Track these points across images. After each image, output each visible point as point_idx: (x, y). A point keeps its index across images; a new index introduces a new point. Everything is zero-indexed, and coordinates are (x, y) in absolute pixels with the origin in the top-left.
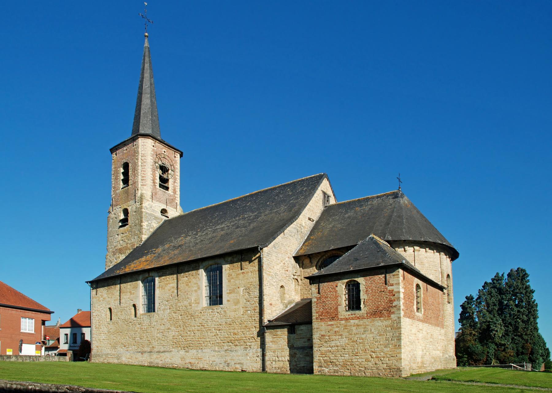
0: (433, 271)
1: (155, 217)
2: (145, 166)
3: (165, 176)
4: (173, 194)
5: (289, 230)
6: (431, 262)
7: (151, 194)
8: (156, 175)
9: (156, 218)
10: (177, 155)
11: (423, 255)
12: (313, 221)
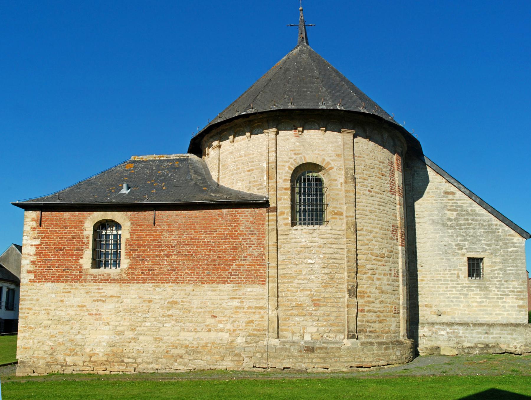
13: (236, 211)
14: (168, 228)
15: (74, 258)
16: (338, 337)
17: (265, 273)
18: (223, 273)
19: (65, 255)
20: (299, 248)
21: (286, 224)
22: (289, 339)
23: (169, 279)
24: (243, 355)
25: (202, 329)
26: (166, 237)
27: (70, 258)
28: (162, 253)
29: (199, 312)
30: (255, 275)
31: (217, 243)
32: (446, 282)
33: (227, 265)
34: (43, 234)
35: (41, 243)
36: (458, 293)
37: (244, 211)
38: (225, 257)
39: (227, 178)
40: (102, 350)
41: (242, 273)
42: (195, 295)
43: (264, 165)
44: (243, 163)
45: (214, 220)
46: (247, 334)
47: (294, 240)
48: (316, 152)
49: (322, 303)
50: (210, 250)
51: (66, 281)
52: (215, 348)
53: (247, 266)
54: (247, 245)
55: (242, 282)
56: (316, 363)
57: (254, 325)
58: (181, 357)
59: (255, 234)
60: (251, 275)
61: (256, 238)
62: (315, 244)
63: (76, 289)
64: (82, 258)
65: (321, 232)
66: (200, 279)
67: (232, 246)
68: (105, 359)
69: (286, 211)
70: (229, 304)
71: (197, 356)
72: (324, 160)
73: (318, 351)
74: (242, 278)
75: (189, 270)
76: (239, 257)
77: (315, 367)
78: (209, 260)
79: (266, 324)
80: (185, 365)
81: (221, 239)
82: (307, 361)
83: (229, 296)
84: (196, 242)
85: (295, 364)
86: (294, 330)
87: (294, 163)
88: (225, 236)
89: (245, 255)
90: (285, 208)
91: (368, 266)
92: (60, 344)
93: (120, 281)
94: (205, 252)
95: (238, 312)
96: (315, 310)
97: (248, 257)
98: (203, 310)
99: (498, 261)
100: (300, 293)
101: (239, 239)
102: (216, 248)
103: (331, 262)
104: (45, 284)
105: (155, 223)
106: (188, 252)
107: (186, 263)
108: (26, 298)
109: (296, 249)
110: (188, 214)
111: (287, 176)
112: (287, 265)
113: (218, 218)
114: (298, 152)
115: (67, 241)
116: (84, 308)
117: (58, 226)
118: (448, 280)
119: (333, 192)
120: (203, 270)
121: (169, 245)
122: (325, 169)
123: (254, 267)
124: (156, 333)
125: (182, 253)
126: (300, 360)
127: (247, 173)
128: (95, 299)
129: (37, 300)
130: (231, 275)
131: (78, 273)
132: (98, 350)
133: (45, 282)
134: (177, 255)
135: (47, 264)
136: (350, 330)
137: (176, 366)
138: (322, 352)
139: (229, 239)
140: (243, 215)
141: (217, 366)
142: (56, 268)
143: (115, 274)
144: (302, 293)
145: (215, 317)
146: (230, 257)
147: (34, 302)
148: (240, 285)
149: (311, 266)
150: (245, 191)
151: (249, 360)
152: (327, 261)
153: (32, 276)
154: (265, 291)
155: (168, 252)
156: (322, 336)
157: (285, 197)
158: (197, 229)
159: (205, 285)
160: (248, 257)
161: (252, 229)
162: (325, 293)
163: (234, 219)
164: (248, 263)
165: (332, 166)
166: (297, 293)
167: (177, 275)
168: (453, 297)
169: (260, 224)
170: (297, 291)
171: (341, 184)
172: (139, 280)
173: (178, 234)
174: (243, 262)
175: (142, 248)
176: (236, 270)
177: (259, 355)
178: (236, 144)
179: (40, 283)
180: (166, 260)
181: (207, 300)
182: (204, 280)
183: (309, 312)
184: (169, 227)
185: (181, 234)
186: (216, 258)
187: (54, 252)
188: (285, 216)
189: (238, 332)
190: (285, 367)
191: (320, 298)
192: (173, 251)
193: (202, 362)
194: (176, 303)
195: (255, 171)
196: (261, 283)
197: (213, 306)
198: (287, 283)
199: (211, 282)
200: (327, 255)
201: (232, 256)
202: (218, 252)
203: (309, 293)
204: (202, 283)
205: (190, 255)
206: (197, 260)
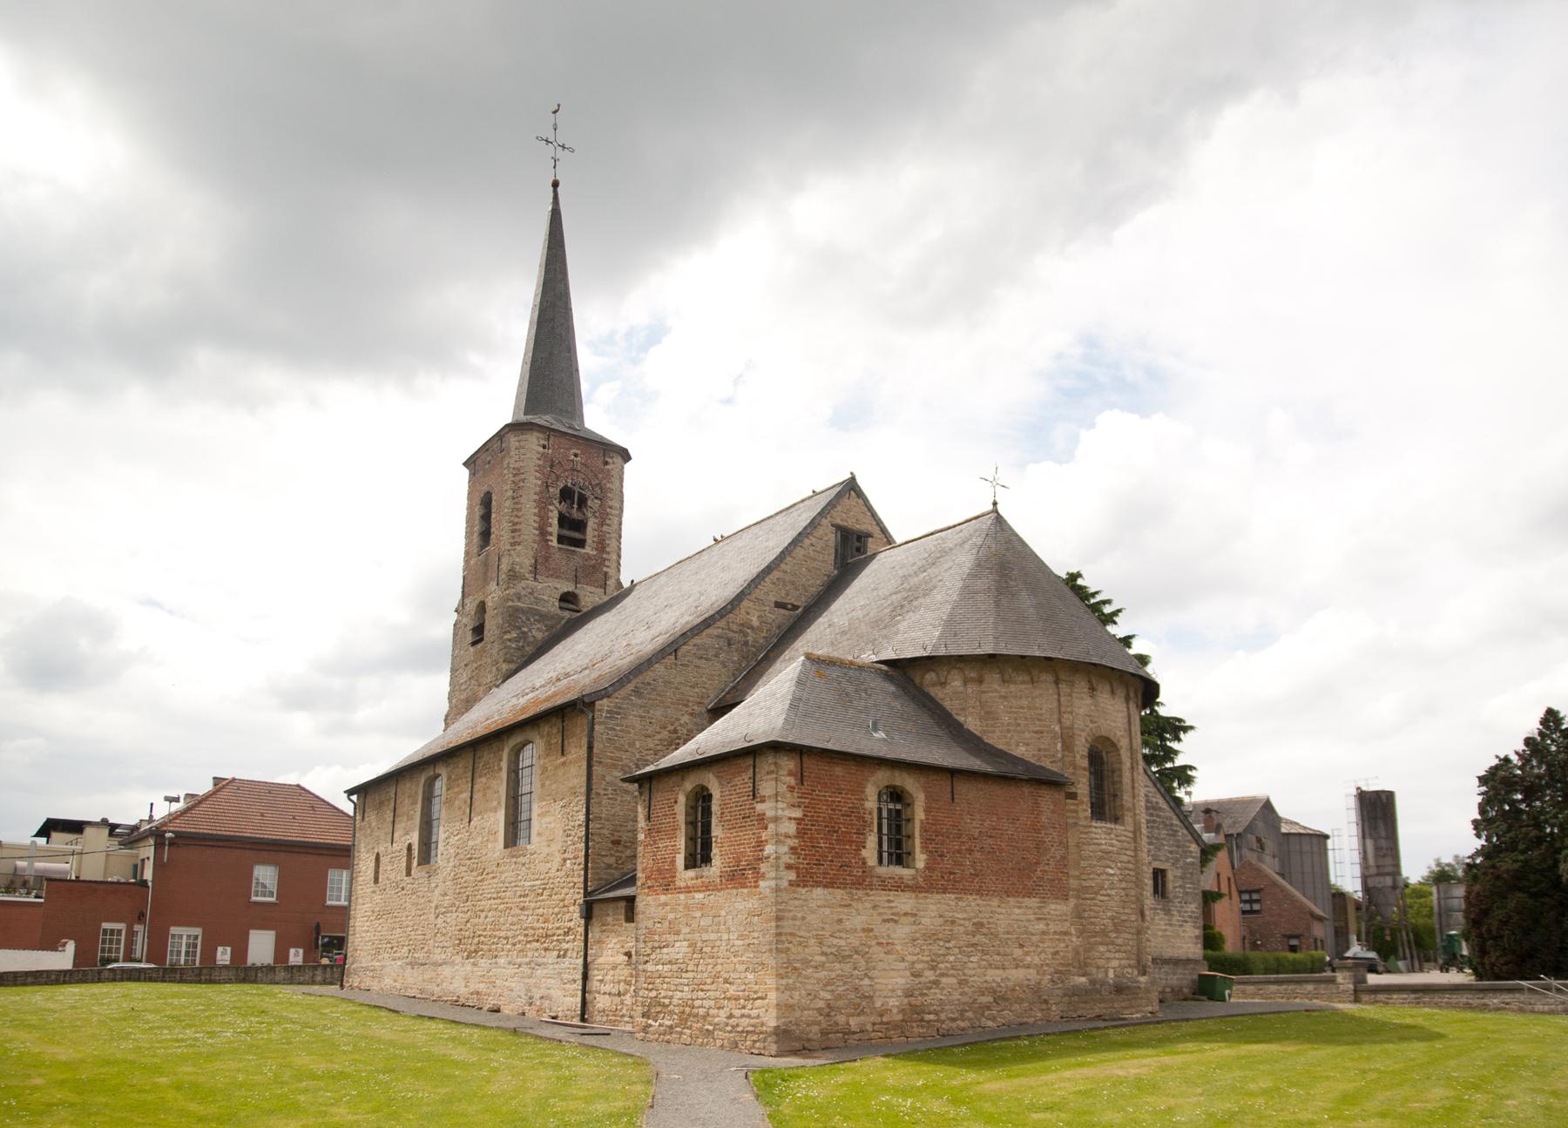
0: (1027, 735)
1: (541, 616)
2: (521, 496)
3: (575, 514)
4: (595, 553)
5: (694, 645)
6: (1023, 708)
7: (533, 561)
8: (550, 514)
9: (543, 617)
10: (612, 458)
11: (996, 691)
12: (795, 607)
15: (854, 847)
19: (840, 840)
21: (1086, 818)
27: (847, 847)
28: (964, 848)
34: (807, 801)
35: (804, 815)
39: (998, 734)
40: (896, 1003)
44: (1026, 719)
50: (1014, 846)
51: (843, 886)
63: (860, 899)
64: (864, 847)
68: (900, 1017)
70: (1037, 927)
72: (1116, 734)
79: (1070, 955)
92: (839, 997)
93: (915, 888)
96: (1116, 938)
99: (1179, 874)
104: (814, 889)
105: (953, 799)
108: (786, 915)
115: (843, 815)
116: (871, 934)
117: (828, 787)
124: (961, 973)
128: (886, 917)
129: (803, 918)
131: (860, 874)
132: (891, 1004)
133: (813, 886)
135: (814, 855)
142: (829, 863)
143: (909, 877)
147: (798, 923)
153: (792, 876)
172: (939, 889)
174: (1046, 868)
175: (940, 837)
179: (806, 889)
187: (824, 834)
188: (1084, 807)
195: (1045, 734)
200: (1124, 865)
204: (1008, 896)
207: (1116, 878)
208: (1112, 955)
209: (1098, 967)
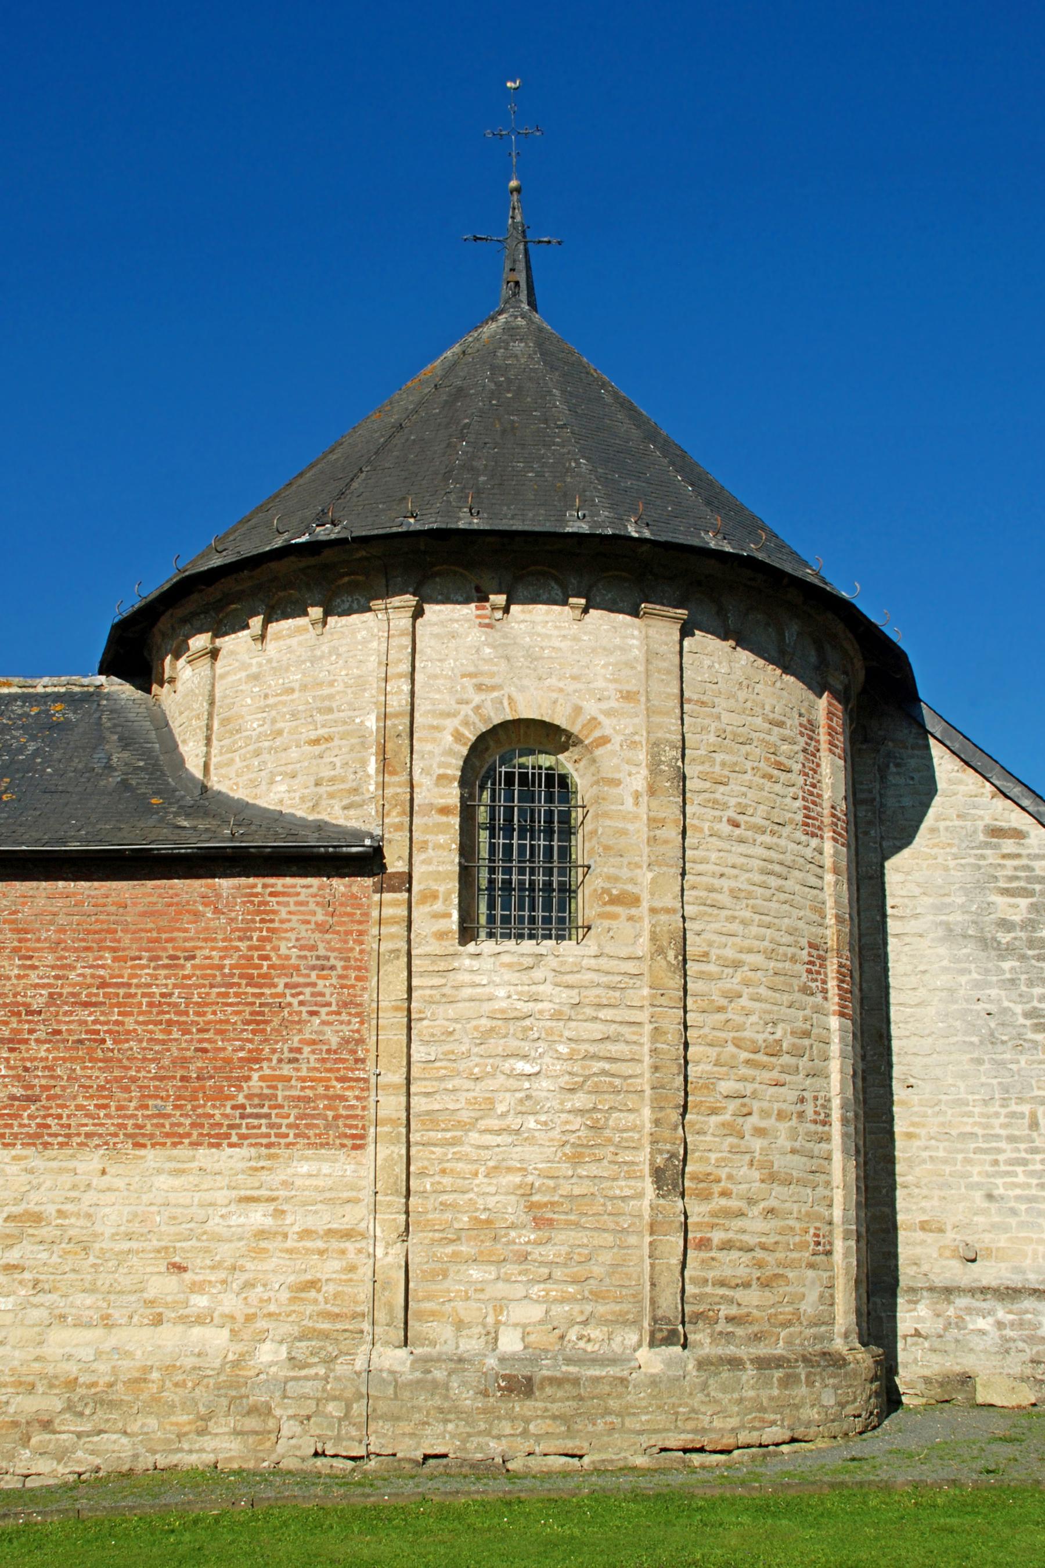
6: (293, 690)
13: (265, 886)
14: (16, 944)
16: (619, 1339)
17: (364, 1108)
18: (214, 1106)
20: (484, 1021)
21: (441, 935)
22: (445, 1349)
23: (16, 1129)
24: (278, 1412)
25: (131, 1317)
26: (9, 978)
29: (122, 1252)
30: (330, 1114)
31: (196, 999)
32: (994, 1145)
33: (228, 1079)
36: (1034, 1181)
37: (294, 886)
38: (224, 1049)
39: (238, 764)
41: (281, 1107)
42: (109, 1189)
43: (368, 724)
44: (294, 715)
45: (186, 917)
46: (296, 1330)
47: (467, 992)
48: (553, 681)
49: (563, 1217)
50: (170, 1023)
52: (176, 1385)
53: (299, 1085)
54: (304, 1009)
55: (283, 1141)
56: (538, 1438)
57: (321, 1299)
58: (47, 1425)
59: (332, 968)
60: (313, 1117)
61: (334, 981)
62: (540, 1006)
65: (563, 963)
66: (130, 1130)
67: (248, 1009)
69: (442, 889)
70: (234, 1220)
71: (108, 1420)
72: (578, 710)
73: (549, 1391)
74: (280, 1126)
75: (91, 1097)
76: (274, 1051)
77: (537, 1450)
78: (166, 1062)
79: (364, 1292)
80: (61, 1455)
81: (212, 986)
82: (508, 1431)
83: (234, 1194)
84: (117, 995)
85: (464, 1442)
86: (463, 1314)
87: (473, 718)
88: (224, 975)
89: (296, 1045)
90: (437, 876)
91: (726, 1086)
94: (151, 1032)
95: (265, 1250)
97: (307, 1049)
98: (134, 1245)
100: (486, 1180)
101: (275, 986)
102: (192, 1017)
103: (595, 1070)
106: (87, 1032)
107: (79, 1072)
109: (474, 1023)
110: (93, 893)
111: (447, 765)
112: (442, 1079)
113: (201, 908)
114: (487, 681)
118: (998, 1136)
119: (608, 822)
120: (143, 1096)
121: (18, 1004)
122: (581, 742)
123: (327, 1088)
125: (65, 1035)
126: (483, 1426)
127: (307, 748)
130: (242, 1117)
134: (50, 1041)
136: (660, 1313)
137: (25, 1460)
138: (560, 1394)
139: (239, 985)
140: (292, 900)
141: (180, 1455)
144: (494, 1181)
145: (181, 1269)
146: (242, 1049)
148: (272, 1151)
149: (527, 1085)
150: (300, 813)
151: (298, 1430)
152: (583, 1068)
154: (363, 1173)
155: (13, 1030)
156: (562, 1337)
157: (442, 839)
158: (124, 949)
159: (149, 1153)
160: (307, 1049)
161: (322, 952)
162: (573, 1181)
163: (259, 912)
164: (304, 1073)
165: (608, 731)
166: (477, 1181)
167: (45, 1117)
168: (1018, 1198)
169: (348, 933)
170: (476, 1174)
171: (637, 795)
173: (53, 967)
174: (287, 1070)
176: (260, 1096)
177: (333, 1409)
178: (272, 646)
180: (7, 1060)
181: (154, 1209)
182: (144, 1135)
183: (516, 1247)
184: (20, 941)
185: (63, 967)
186: (189, 1054)
189: (261, 1324)
190: (429, 1452)
191: (556, 1199)
192: (32, 1026)
193: (124, 1440)
194: (37, 1218)
195: (336, 742)
196: (349, 1142)
197: (173, 1229)
198: (442, 1145)
199: (169, 1141)
200: (584, 1047)
201: (250, 1046)
202: (200, 1031)
203: (517, 1179)
204: (138, 1145)
205: (95, 1041)
206: (120, 1061)
207: (545, 1084)
208: (520, 1291)
209: (460, 1325)
